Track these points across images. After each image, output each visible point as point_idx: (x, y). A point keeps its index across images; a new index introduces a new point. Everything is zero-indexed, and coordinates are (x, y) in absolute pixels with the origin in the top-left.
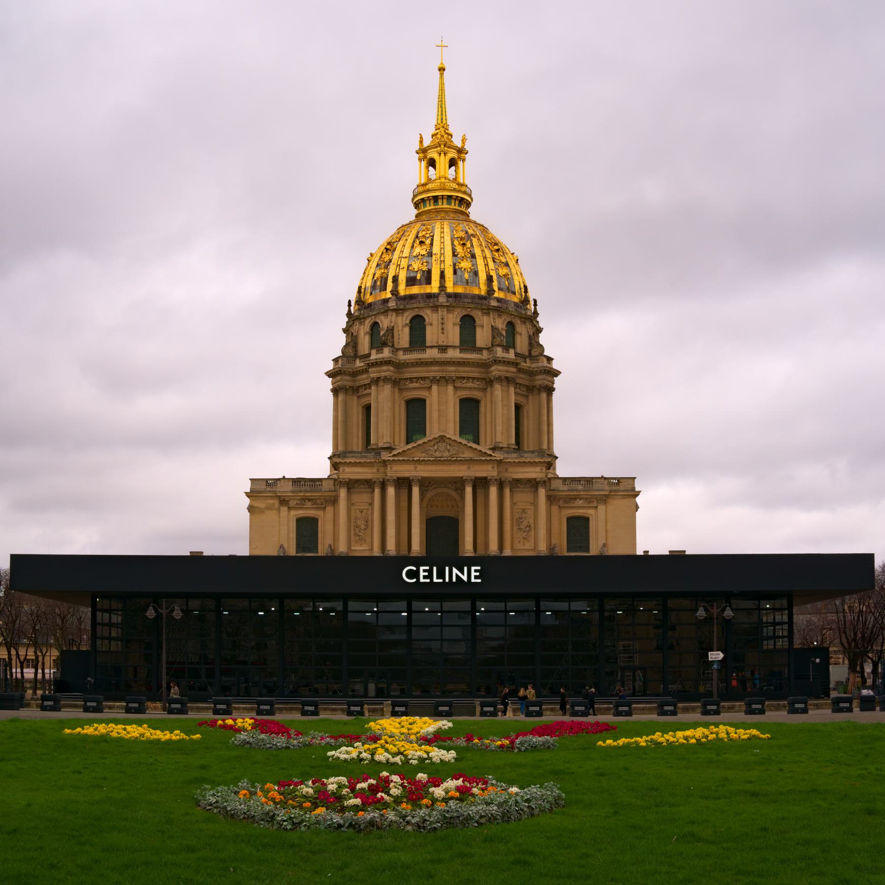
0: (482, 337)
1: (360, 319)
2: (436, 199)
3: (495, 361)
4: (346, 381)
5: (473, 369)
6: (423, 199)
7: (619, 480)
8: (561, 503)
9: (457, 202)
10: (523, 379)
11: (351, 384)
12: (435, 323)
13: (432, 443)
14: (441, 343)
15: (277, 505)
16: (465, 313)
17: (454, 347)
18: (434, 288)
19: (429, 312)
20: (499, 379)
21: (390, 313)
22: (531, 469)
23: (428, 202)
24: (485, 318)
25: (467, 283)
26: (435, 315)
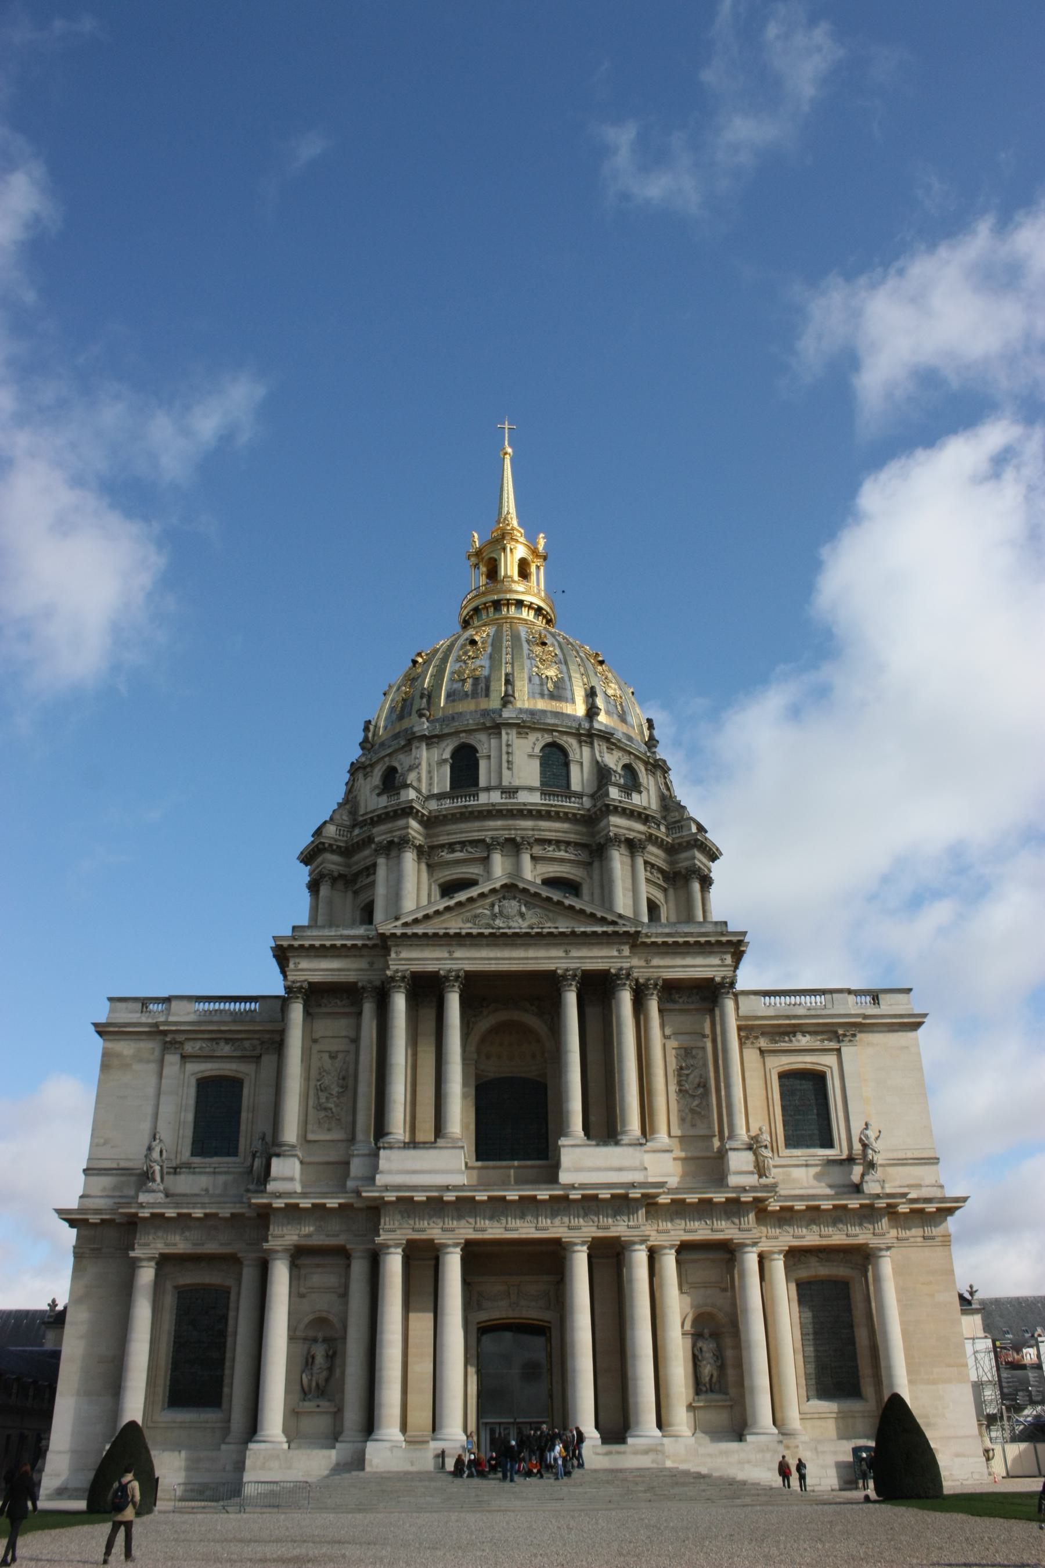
0: (579, 778)
1: (365, 768)
2: (497, 605)
3: (608, 806)
4: (332, 862)
5: (566, 826)
6: (476, 610)
7: (875, 996)
8: (763, 1043)
9: (532, 613)
10: (656, 856)
11: (342, 870)
12: (494, 754)
13: (489, 901)
14: (505, 783)
15: (157, 1052)
16: (550, 740)
17: (531, 789)
18: (495, 703)
19: (482, 737)
20: (617, 841)
21: (415, 744)
22: (699, 961)
23: (484, 613)
24: (586, 750)
25: (553, 697)
26: (494, 742)
